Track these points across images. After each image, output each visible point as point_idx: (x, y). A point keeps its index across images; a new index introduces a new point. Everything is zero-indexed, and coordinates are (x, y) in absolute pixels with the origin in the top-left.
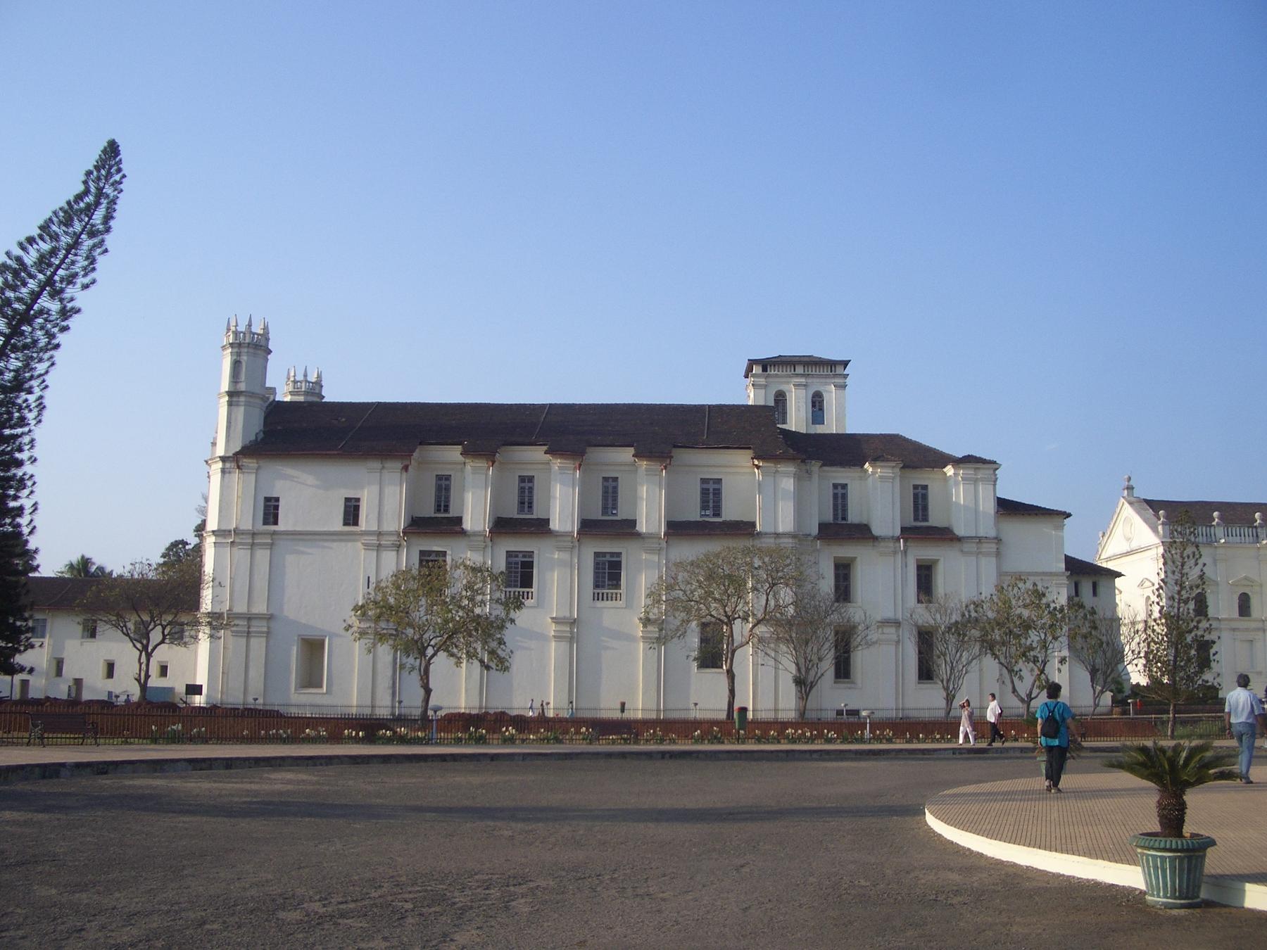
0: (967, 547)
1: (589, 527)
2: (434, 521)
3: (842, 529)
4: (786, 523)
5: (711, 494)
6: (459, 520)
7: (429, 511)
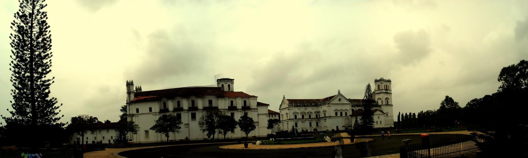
1: (190, 109)
2: (164, 110)
3: (232, 108)
4: (223, 108)
5: (210, 102)
6: (168, 109)
7: (163, 108)
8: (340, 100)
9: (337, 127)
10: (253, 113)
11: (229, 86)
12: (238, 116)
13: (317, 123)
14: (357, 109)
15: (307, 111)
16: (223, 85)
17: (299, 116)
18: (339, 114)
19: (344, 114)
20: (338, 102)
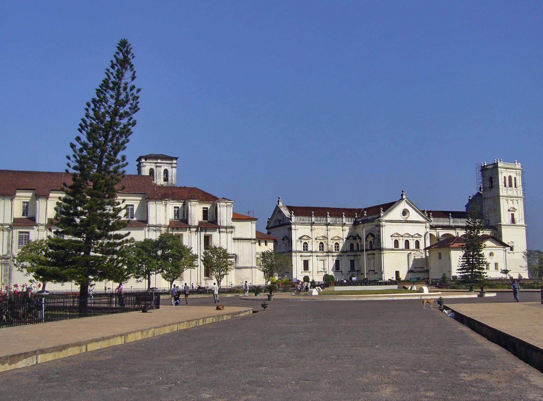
0: (221, 230)
8: (405, 212)
9: (397, 273)
10: (223, 235)
11: (166, 172)
12: (192, 241)
13: (352, 262)
14: (442, 232)
15: (315, 235)
16: (152, 171)
17: (314, 246)
18: (402, 245)
19: (412, 245)
20: (400, 217)
